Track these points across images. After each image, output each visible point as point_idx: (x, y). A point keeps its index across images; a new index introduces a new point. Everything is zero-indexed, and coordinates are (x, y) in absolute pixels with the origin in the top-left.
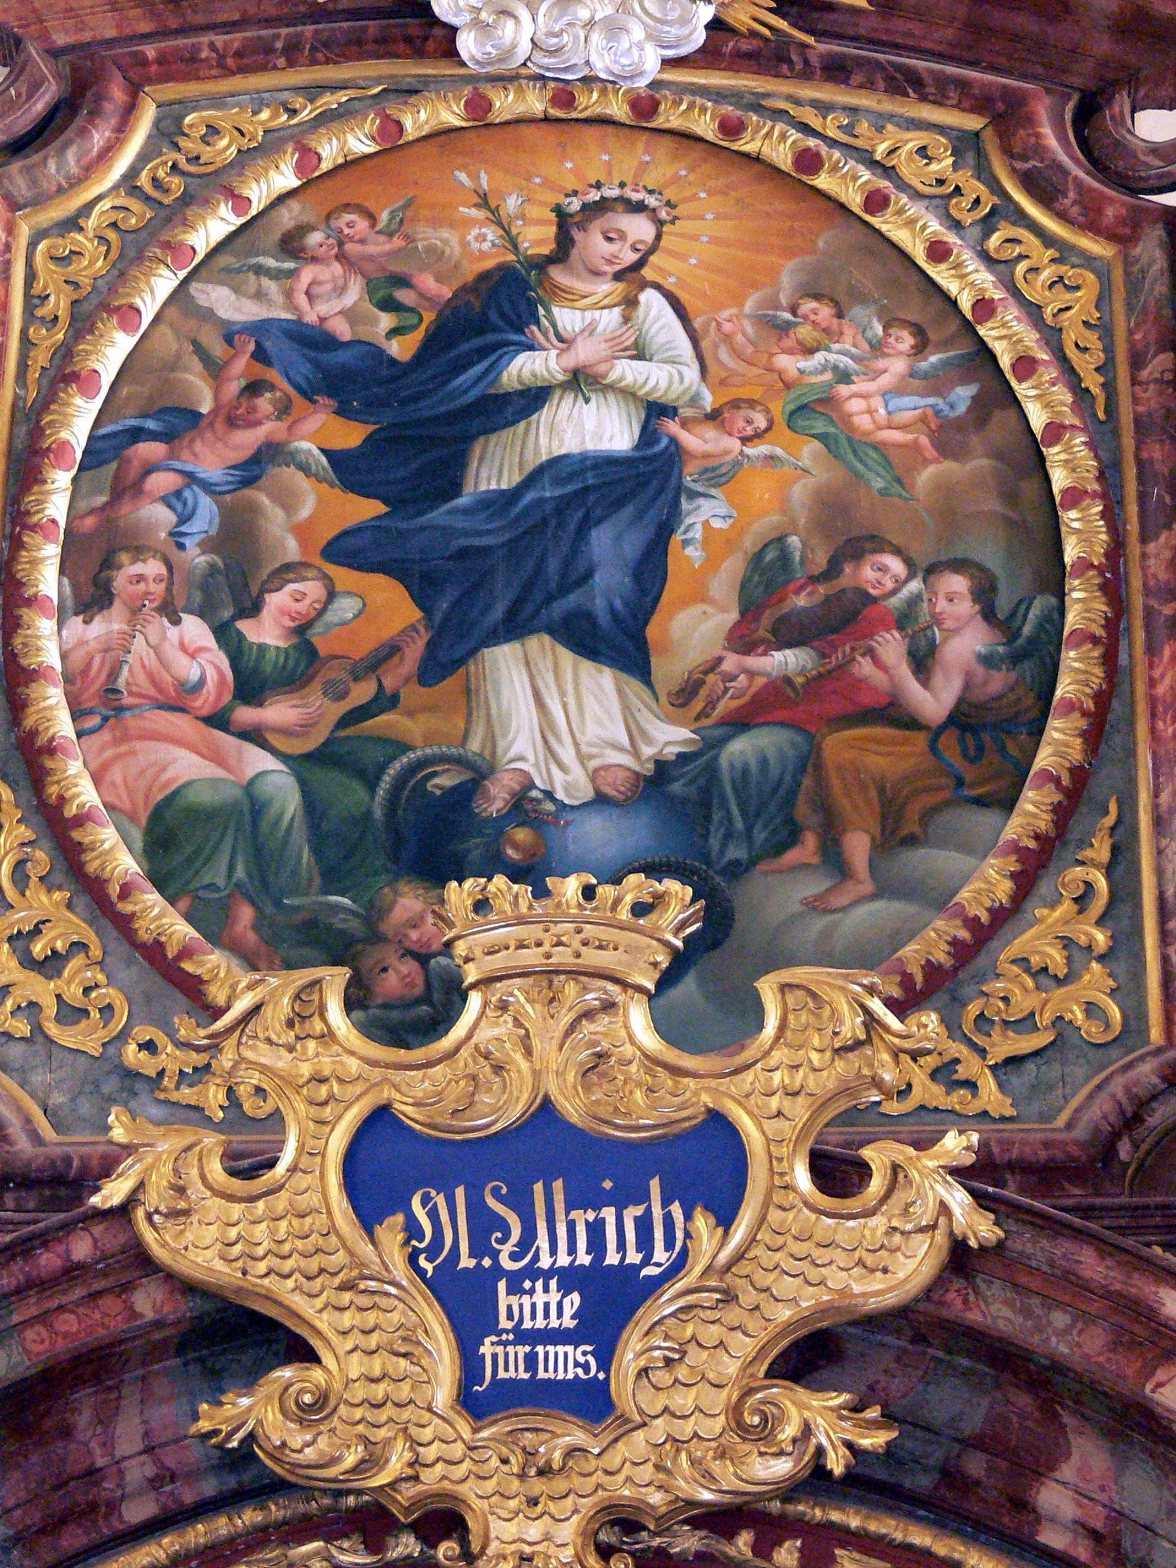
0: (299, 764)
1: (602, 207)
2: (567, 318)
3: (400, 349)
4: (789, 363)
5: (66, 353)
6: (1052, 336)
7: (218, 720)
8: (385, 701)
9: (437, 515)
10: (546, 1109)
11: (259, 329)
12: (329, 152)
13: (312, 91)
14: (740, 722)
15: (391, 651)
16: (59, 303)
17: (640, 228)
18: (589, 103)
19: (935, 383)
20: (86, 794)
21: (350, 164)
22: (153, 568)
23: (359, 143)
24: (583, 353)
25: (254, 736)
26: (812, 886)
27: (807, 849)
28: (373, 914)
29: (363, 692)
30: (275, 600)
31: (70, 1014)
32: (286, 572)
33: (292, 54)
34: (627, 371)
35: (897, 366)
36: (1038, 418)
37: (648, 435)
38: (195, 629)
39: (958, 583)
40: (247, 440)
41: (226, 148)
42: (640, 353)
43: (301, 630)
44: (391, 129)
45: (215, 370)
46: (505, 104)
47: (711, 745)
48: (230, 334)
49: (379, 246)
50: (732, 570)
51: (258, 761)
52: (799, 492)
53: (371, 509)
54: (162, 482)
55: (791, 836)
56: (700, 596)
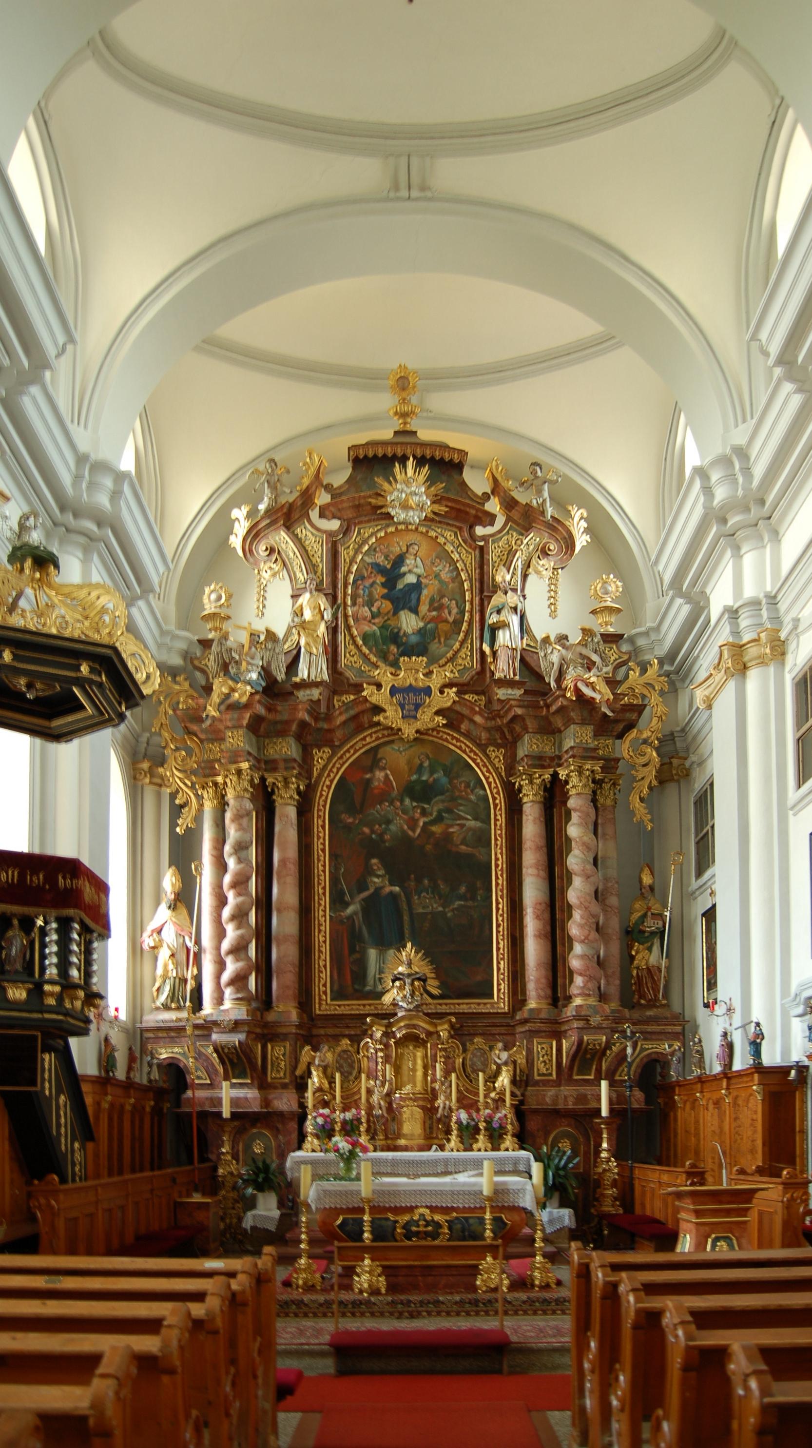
0: (379, 628)
1: (411, 544)
2: (408, 561)
3: (389, 567)
4: (434, 569)
5: (349, 568)
6: (465, 565)
7: (370, 622)
8: (389, 619)
9: (394, 592)
10: (411, 685)
11: (372, 563)
12: (379, 536)
13: (376, 526)
14: (429, 622)
15: (389, 612)
16: (348, 560)
17: (416, 547)
18: (410, 527)
19: (451, 571)
20: (356, 633)
21: (381, 537)
22: (361, 600)
23: (382, 534)
24: (410, 567)
25: (374, 624)
26: (437, 645)
27: (437, 640)
28: (388, 649)
29: (386, 618)
30: (376, 604)
31: (355, 662)
32: (377, 600)
33: (374, 520)
34: (415, 570)
35: (447, 569)
36: (464, 578)
37: (418, 580)
38: (366, 608)
39: (454, 602)
40: (371, 581)
41: (366, 535)
42: (417, 567)
43: (379, 609)
44: (386, 532)
45: (367, 570)
46: (400, 527)
47: (426, 625)
48: (368, 564)
49: (386, 551)
50: (428, 600)
51: (375, 628)
52: (436, 588)
53: (386, 591)
54: (361, 587)
55: (434, 638)
56: (424, 604)
